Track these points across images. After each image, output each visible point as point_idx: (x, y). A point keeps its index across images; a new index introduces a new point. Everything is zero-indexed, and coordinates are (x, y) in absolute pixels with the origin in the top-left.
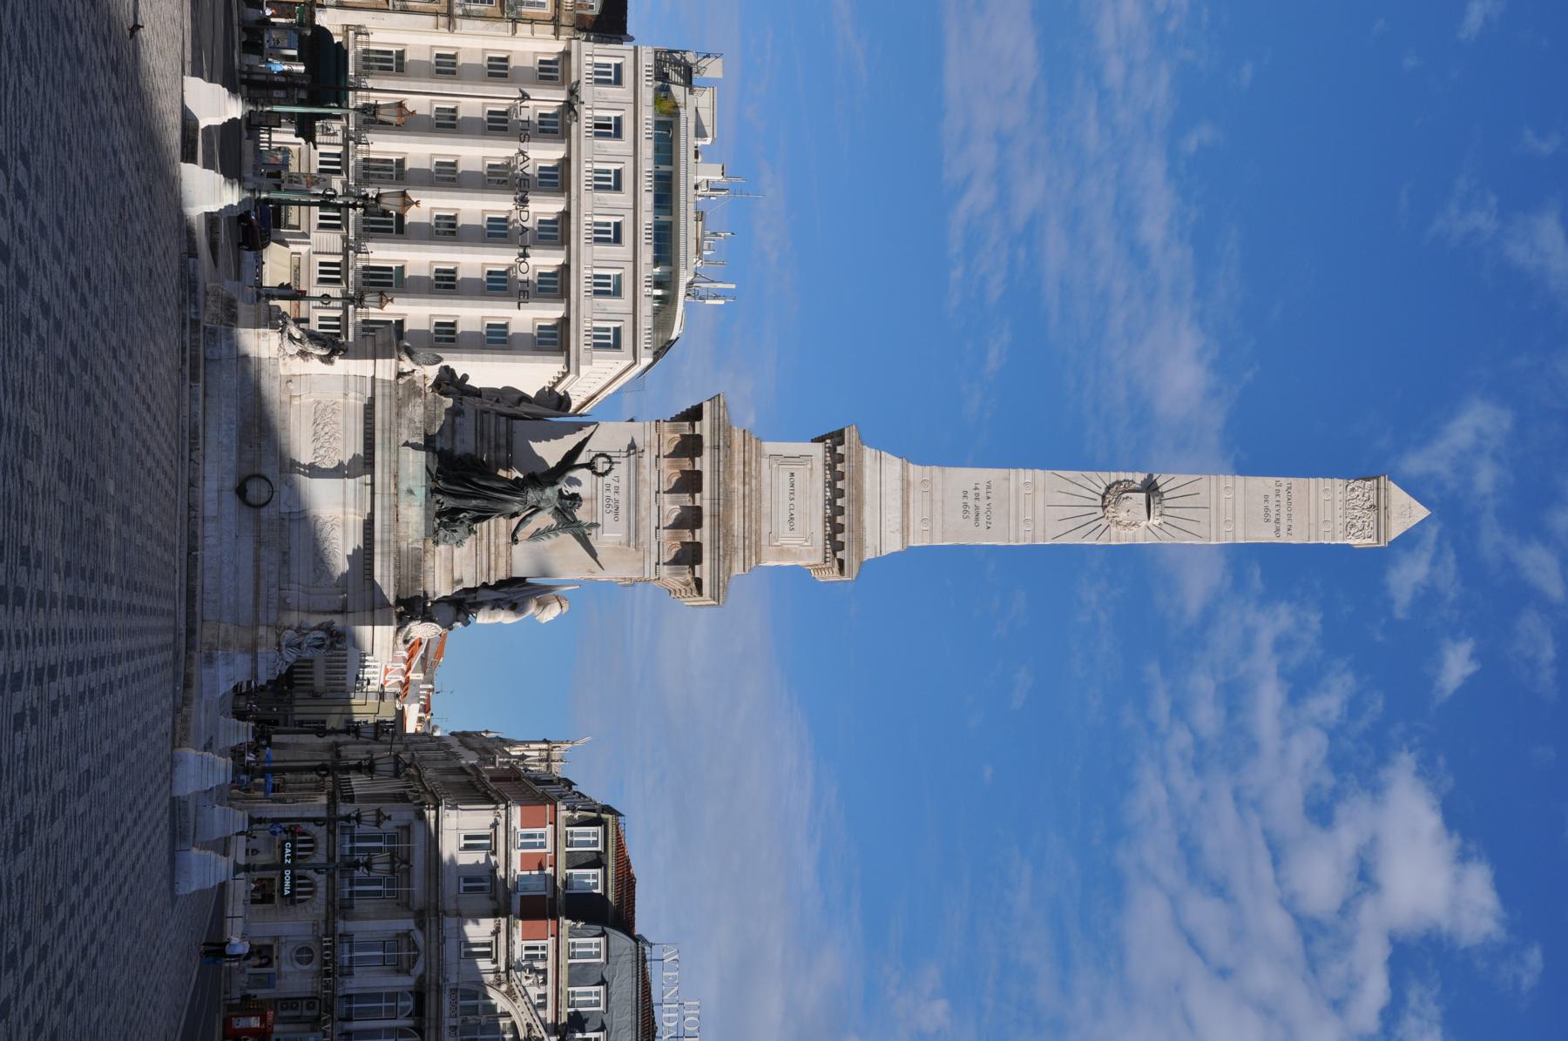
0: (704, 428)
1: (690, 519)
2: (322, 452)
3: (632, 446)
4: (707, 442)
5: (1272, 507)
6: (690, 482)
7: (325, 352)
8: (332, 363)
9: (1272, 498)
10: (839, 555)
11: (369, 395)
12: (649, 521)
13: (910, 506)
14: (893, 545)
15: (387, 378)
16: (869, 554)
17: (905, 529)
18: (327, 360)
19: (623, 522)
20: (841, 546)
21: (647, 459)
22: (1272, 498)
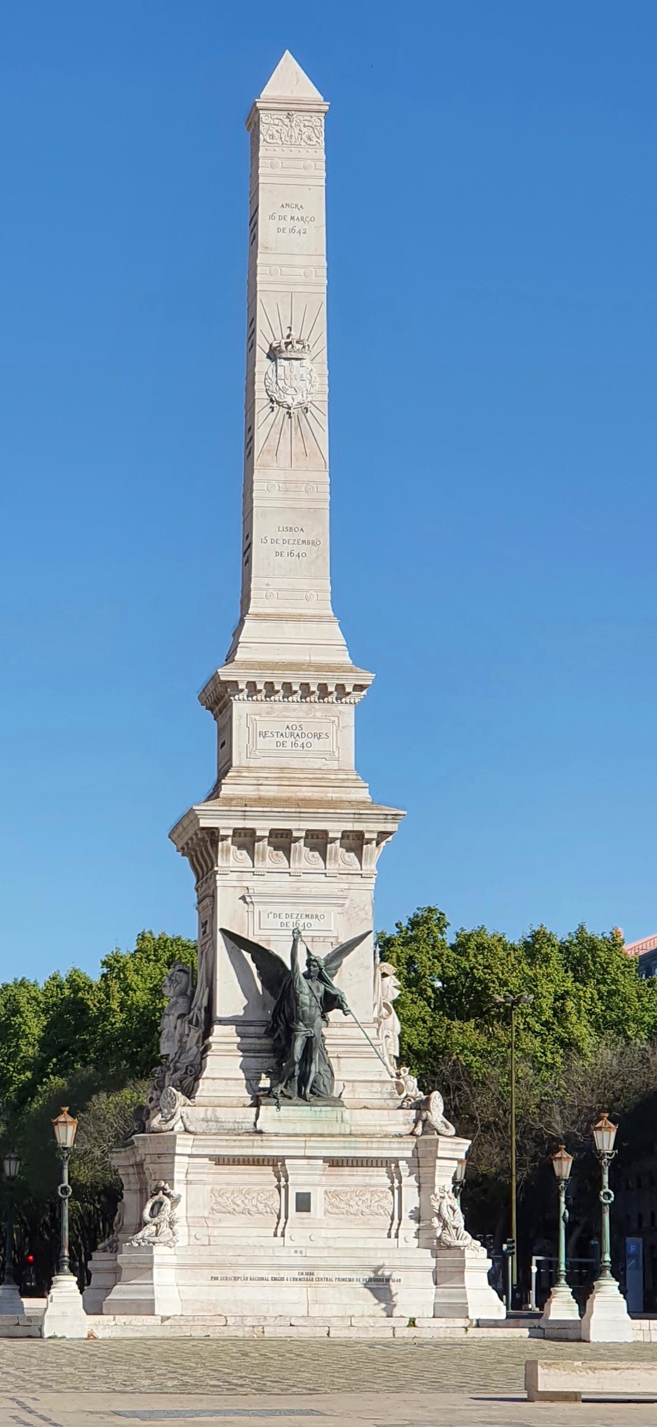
0: (226, 826)
1: (318, 841)
2: (261, 1206)
3: (243, 898)
4: (240, 824)
5: (287, 224)
6: (282, 841)
7: (167, 1201)
8: (180, 1196)
9: (282, 224)
10: (349, 689)
11: (206, 1160)
12: (318, 885)
13: (292, 611)
14: (334, 632)
15: (191, 1143)
16: (345, 658)
17: (318, 619)
18: (176, 1201)
19: (320, 910)
20: (340, 688)
21: (254, 884)
22: (282, 224)
